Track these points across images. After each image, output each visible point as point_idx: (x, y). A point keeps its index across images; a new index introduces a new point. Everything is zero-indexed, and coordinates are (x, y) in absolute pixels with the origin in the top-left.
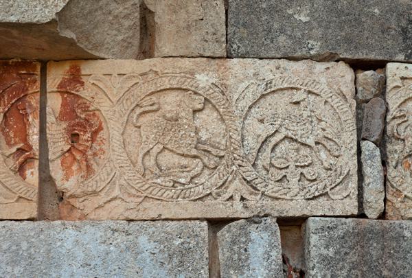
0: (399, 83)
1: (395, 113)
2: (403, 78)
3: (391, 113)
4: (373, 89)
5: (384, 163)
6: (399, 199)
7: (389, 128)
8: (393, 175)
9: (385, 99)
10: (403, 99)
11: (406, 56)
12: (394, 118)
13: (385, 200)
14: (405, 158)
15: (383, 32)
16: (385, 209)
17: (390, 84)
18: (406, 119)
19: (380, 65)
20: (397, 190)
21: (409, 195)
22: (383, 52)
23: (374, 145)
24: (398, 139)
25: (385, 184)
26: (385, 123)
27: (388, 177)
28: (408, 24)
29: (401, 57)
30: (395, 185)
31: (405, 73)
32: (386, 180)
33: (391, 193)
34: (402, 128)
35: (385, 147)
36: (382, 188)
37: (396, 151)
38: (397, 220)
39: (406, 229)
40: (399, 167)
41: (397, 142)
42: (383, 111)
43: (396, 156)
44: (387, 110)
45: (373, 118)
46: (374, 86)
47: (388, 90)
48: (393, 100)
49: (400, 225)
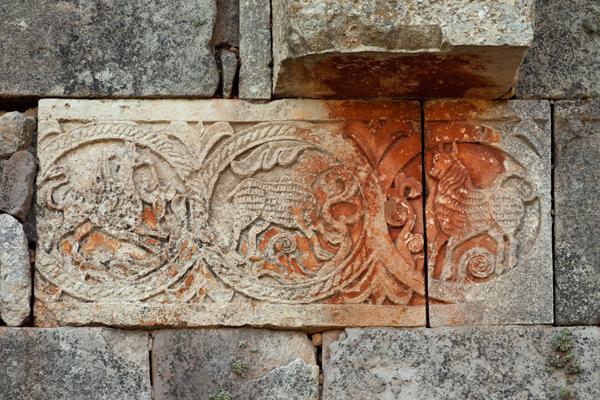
0: (56, 128)
1: (48, 172)
2: (62, 121)
3: (43, 172)
4: (16, 139)
5: (32, 246)
6: (54, 297)
7: (40, 194)
8: (44, 262)
9: (35, 154)
10: (61, 152)
11: (66, 89)
12: (48, 179)
13: (32, 300)
14: (65, 236)
15: (31, 55)
16: (32, 312)
17: (42, 131)
18: (65, 181)
19: (27, 104)
20: (51, 283)
21: (68, 290)
22: (31, 83)
23: (14, 220)
24: (54, 210)
25: (33, 277)
26: (34, 187)
27: (37, 265)
28: (70, 42)
29: (60, 90)
30: (47, 277)
31: (64, 114)
32: (33, 270)
33: (42, 288)
34: (59, 194)
35: (35, 222)
36: (26, 281)
37: (50, 228)
38: (52, 326)
39: (63, 339)
40: (55, 250)
41: (51, 214)
42: (30, 169)
43: (51, 234)
44: (37, 169)
45: (15, 181)
46: (17, 134)
47: (39, 140)
48: (47, 154)
49: (54, 333)
